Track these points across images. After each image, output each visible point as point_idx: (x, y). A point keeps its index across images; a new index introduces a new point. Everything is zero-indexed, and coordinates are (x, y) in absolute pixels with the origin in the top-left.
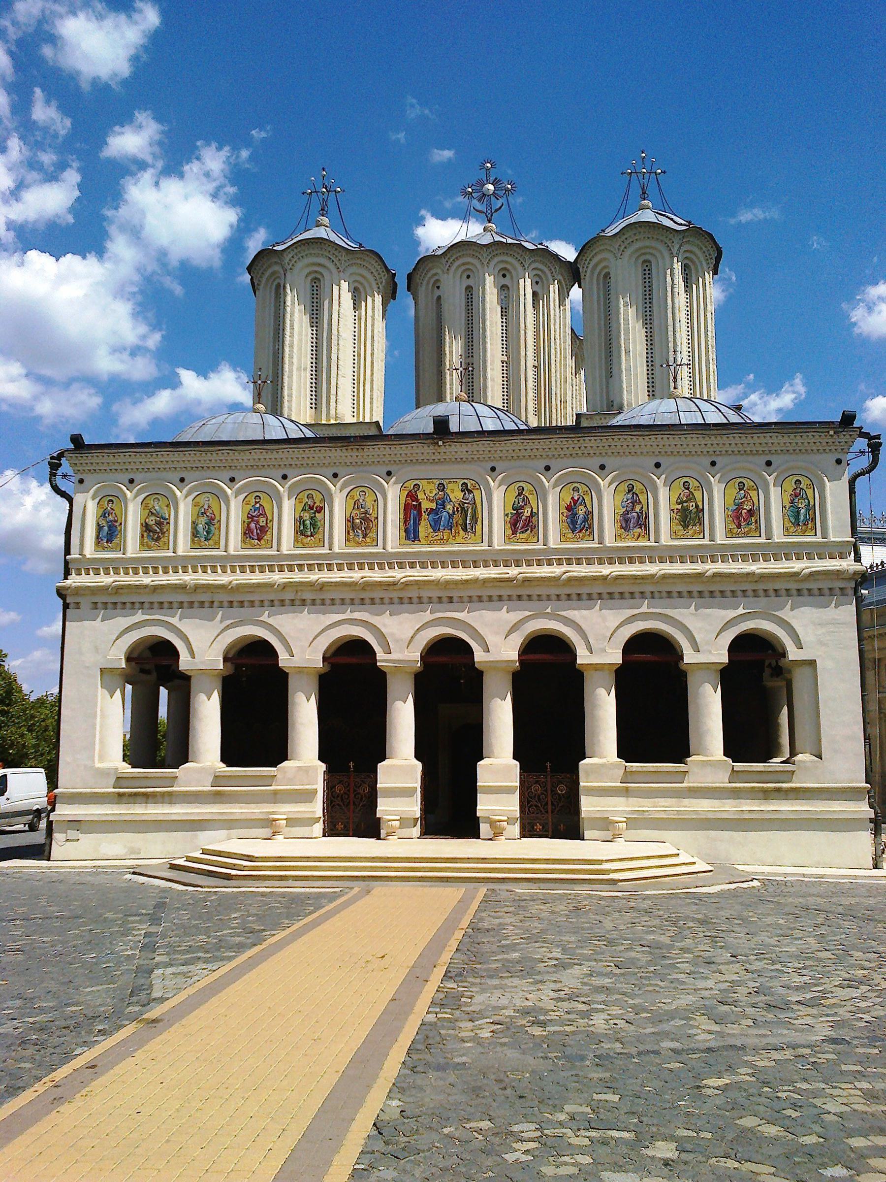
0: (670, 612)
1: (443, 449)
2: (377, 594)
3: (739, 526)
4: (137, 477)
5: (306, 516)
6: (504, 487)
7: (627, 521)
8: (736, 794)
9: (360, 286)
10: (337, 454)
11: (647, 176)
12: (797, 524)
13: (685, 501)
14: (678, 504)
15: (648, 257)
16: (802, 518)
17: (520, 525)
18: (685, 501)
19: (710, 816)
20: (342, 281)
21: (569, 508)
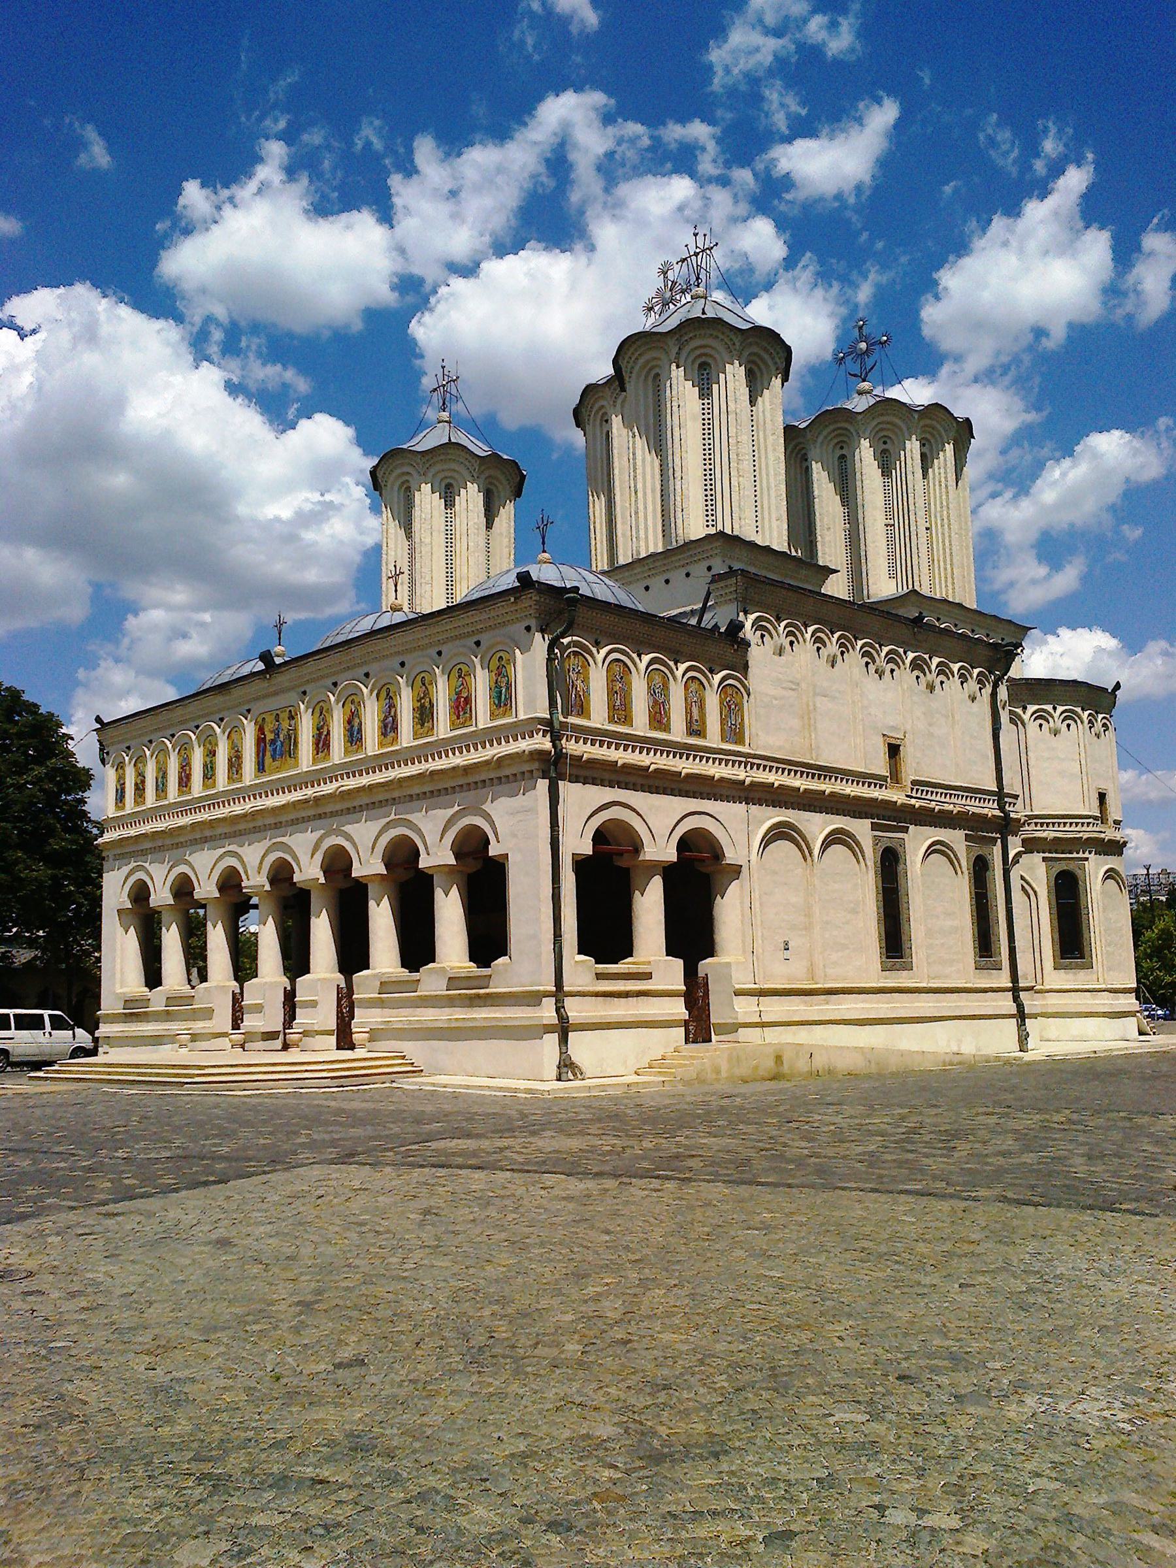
0: (408, 817)
1: (273, 682)
2: (242, 826)
3: (458, 718)
4: (132, 743)
5: (208, 760)
6: (310, 711)
7: (385, 726)
8: (451, 1002)
9: (452, 481)
10: (218, 700)
11: (700, 257)
12: (499, 706)
13: (423, 698)
14: (418, 701)
15: (653, 373)
16: (503, 696)
17: (320, 745)
18: (423, 698)
19: (430, 1025)
20: (423, 485)
21: (349, 722)
